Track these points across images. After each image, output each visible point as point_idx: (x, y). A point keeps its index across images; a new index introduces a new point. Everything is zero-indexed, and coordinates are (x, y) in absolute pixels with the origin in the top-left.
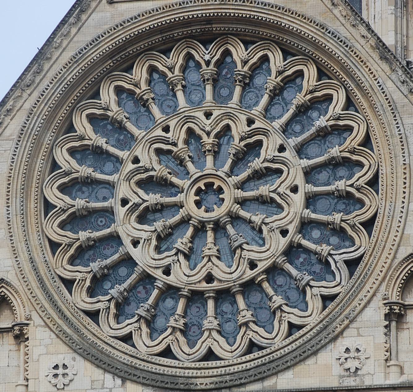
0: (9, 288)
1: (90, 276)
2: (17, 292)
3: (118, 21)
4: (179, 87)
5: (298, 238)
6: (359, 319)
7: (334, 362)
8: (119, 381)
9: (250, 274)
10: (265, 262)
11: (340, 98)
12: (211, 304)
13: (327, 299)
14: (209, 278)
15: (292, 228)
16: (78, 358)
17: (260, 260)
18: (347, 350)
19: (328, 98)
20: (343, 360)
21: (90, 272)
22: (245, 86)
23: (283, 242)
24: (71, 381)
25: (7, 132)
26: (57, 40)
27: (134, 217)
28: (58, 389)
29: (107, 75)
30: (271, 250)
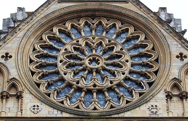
0: (16, 81)
1: (47, 83)
2: (19, 82)
3: (62, 7)
4: (82, 30)
5: (129, 76)
6: (155, 96)
7: (147, 110)
8: (60, 112)
9: (110, 85)
10: (116, 82)
11: (142, 37)
12: (95, 94)
13: (141, 94)
14: (95, 86)
15: (127, 72)
16: (43, 104)
17: (114, 81)
18: (152, 106)
19: (138, 37)
20: (150, 109)
21: (47, 82)
22: (107, 32)
23: (123, 77)
24: (40, 111)
25: (19, 35)
26: (40, 10)
27: (65, 66)
28: (34, 113)
29: (56, 24)
30: (119, 78)
